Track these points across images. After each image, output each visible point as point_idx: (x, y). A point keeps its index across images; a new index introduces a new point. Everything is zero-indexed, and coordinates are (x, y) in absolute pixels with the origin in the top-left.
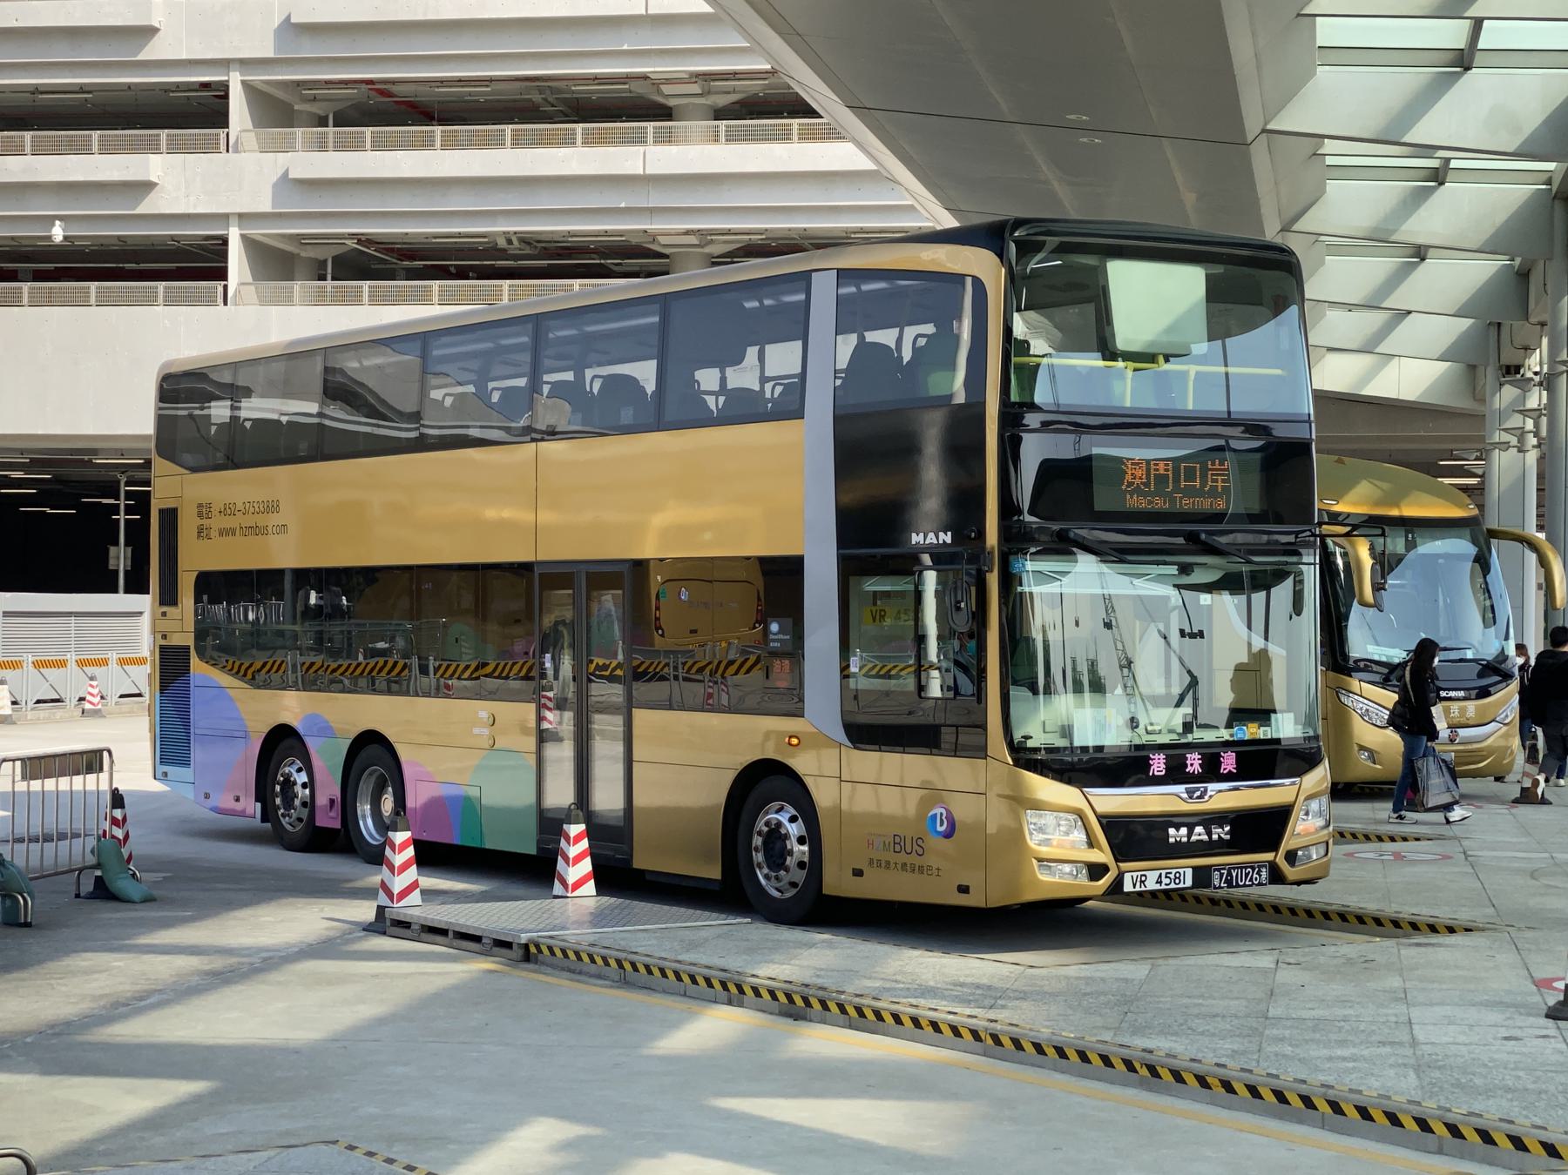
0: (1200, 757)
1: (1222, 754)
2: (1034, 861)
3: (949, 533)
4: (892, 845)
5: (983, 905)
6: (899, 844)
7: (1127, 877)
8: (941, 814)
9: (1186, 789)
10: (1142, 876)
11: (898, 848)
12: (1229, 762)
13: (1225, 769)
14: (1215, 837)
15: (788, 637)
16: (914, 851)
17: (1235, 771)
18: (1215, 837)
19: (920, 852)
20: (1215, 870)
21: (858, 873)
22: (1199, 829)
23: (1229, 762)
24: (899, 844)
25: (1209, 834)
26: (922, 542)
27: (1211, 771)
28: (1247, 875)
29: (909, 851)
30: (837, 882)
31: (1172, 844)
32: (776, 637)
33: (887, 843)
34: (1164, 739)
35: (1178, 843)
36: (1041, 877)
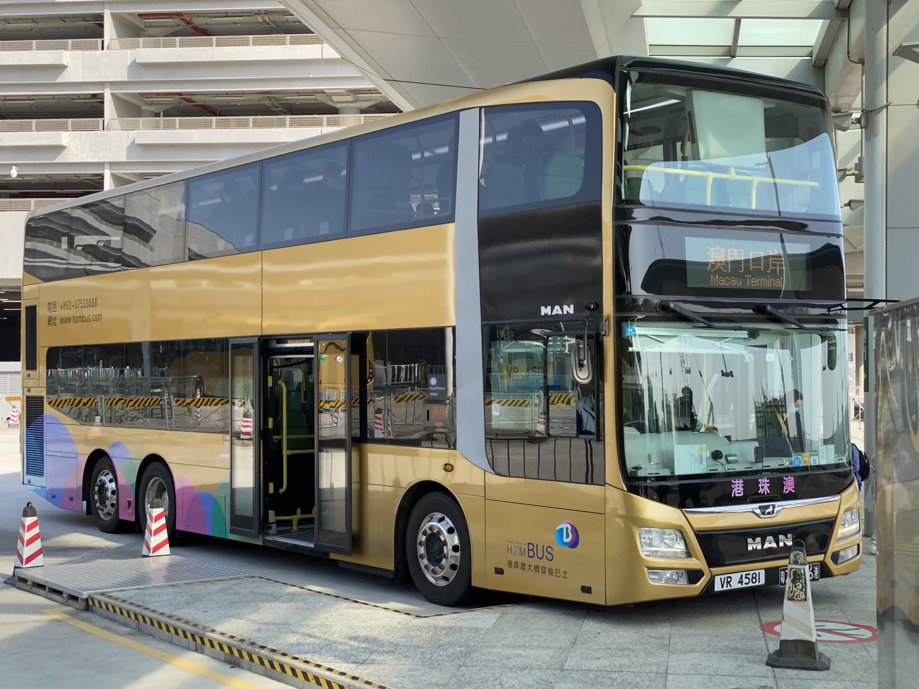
0: (768, 481)
2: (645, 569)
3: (572, 306)
4: (527, 551)
6: (532, 550)
8: (567, 529)
10: (728, 577)
12: (789, 484)
13: (786, 490)
14: (781, 544)
16: (545, 557)
17: (793, 491)
19: (550, 557)
20: (781, 570)
23: (789, 484)
24: (532, 550)
26: (549, 314)
29: (540, 556)
30: (482, 578)
31: (750, 551)
32: (435, 389)
33: (522, 550)
34: (739, 468)
35: (755, 550)
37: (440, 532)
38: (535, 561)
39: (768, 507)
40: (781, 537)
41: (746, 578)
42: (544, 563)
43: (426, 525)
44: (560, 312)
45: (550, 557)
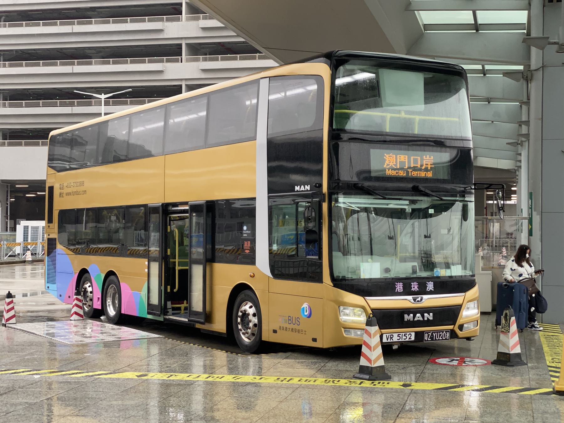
0: (417, 284)
3: (309, 186)
4: (288, 320)
6: (290, 320)
7: (384, 335)
8: (306, 307)
9: (413, 297)
10: (391, 335)
11: (290, 322)
12: (430, 286)
13: (428, 289)
15: (250, 232)
17: (433, 290)
18: (426, 319)
22: (418, 315)
23: (430, 286)
24: (290, 320)
25: (423, 316)
26: (299, 190)
27: (423, 291)
28: (440, 335)
29: (294, 323)
30: (267, 336)
36: (345, 335)
38: (291, 326)
39: (418, 298)
40: (426, 315)
41: (404, 336)
43: (243, 308)
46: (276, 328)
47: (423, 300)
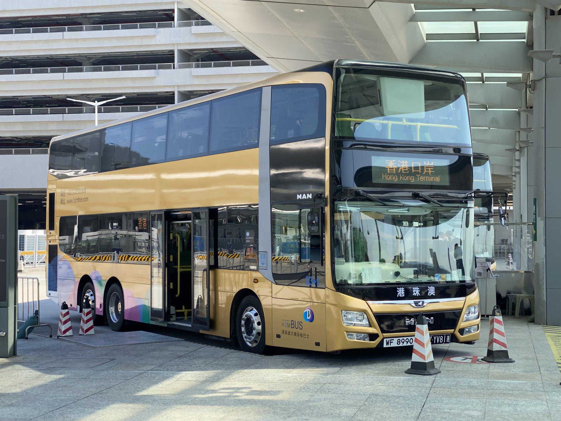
0: (419, 289)
1: (429, 287)
2: (345, 333)
3: (311, 194)
5: (325, 351)
6: (293, 324)
8: (309, 312)
9: (414, 302)
11: (293, 327)
13: (430, 294)
15: (252, 238)
17: (434, 295)
19: (301, 328)
21: (278, 336)
23: (432, 291)
24: (293, 324)
26: (301, 198)
27: (424, 296)
29: (297, 327)
33: (289, 324)
34: (403, 281)
36: (347, 339)
37: (251, 317)
38: (294, 330)
39: (420, 302)
42: (298, 331)
44: (306, 198)
45: (301, 328)
46: (280, 333)
47: (425, 304)
